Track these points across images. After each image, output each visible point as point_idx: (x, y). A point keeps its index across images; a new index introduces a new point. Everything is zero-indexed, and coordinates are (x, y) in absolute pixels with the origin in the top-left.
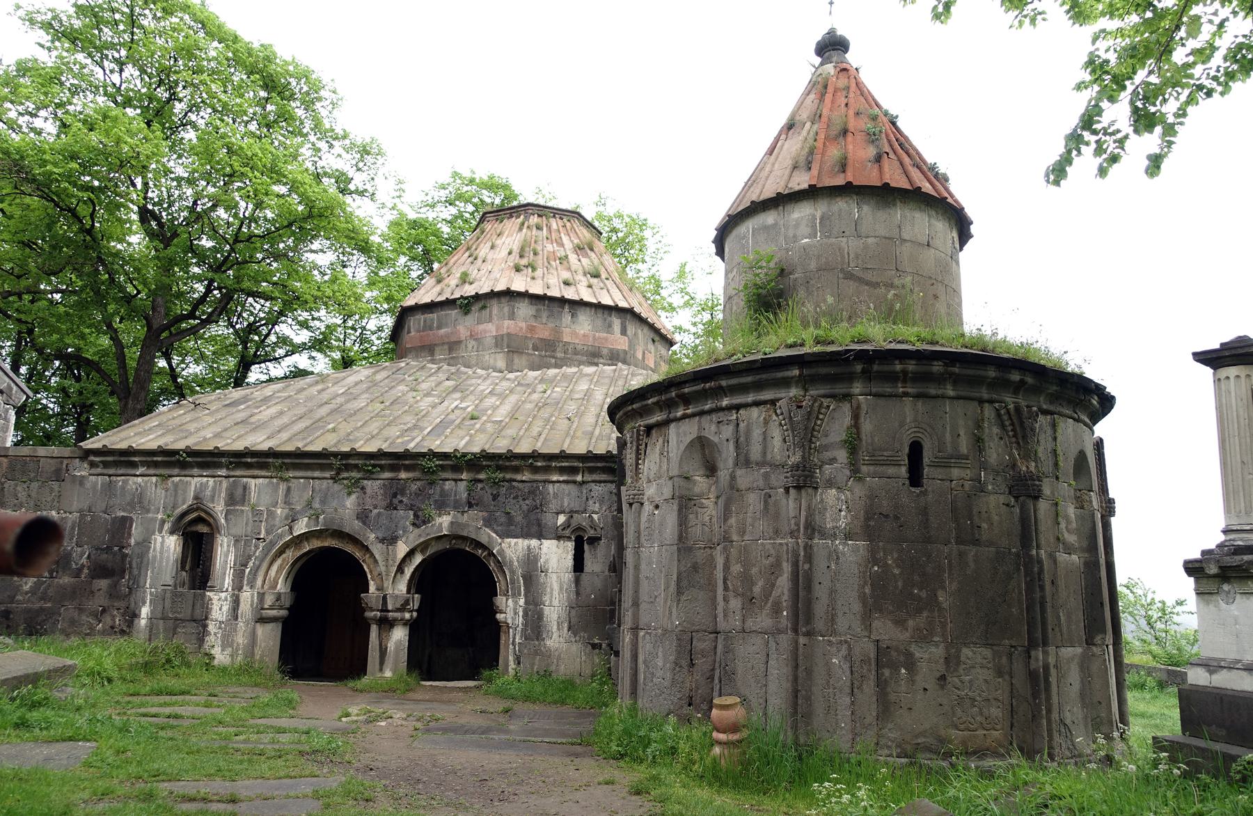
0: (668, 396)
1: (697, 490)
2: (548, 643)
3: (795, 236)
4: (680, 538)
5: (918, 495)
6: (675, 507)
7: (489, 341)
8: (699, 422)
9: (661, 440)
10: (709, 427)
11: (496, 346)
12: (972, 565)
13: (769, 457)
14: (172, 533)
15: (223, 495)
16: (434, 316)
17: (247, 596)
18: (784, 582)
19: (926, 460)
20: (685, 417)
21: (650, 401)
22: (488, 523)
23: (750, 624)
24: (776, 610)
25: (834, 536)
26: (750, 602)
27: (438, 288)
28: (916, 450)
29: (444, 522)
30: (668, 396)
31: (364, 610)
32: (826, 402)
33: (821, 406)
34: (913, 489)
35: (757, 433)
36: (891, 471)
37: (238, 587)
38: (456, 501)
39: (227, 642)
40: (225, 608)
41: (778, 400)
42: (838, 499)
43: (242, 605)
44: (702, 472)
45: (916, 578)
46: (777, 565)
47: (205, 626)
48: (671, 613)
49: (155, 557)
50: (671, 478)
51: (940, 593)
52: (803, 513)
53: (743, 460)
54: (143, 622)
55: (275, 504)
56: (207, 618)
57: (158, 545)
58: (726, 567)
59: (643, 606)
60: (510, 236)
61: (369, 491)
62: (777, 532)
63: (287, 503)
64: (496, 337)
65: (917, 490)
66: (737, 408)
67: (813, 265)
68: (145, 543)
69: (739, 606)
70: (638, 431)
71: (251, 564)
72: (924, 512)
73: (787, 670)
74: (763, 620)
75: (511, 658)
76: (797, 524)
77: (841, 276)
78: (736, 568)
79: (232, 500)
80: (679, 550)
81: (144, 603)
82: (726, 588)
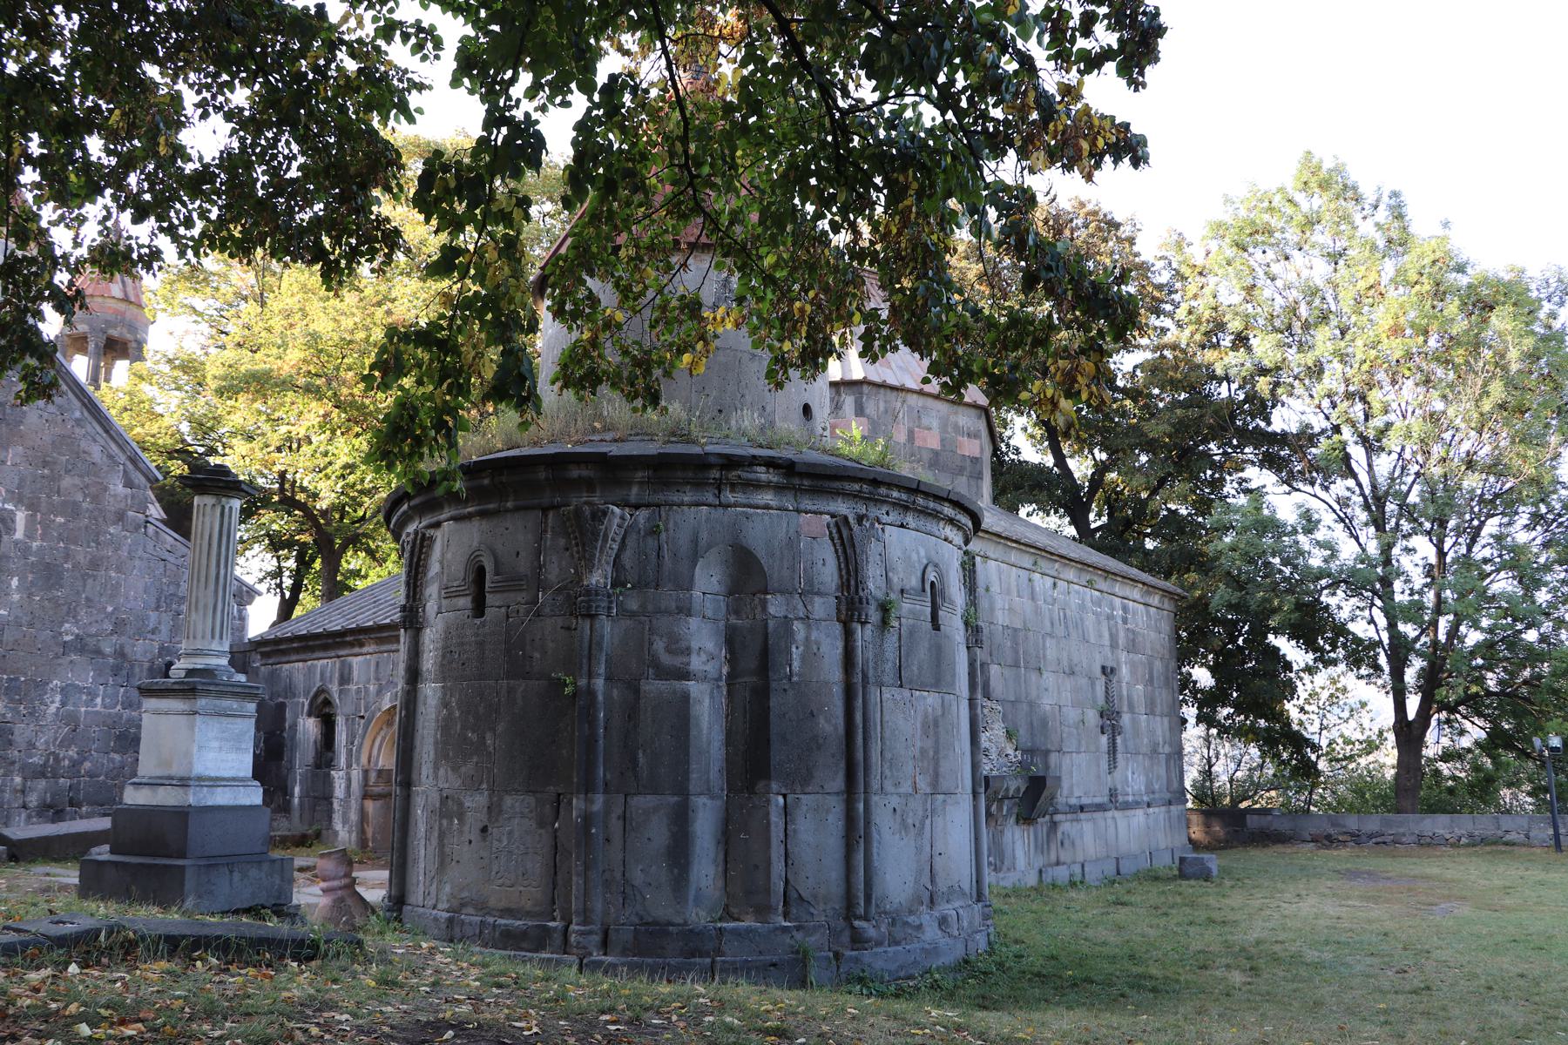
14: (309, 715)
17: (356, 774)
19: (487, 585)
37: (349, 766)
39: (345, 821)
51: (488, 735)
54: (296, 801)
55: (368, 681)
63: (377, 679)
68: (294, 726)
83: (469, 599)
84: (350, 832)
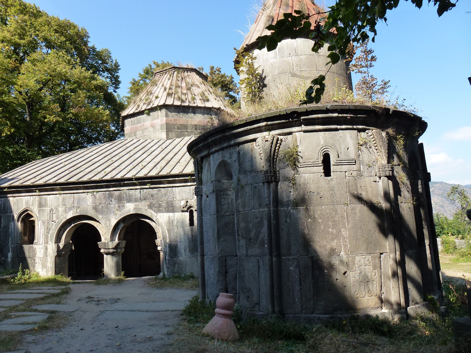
0: (207, 142)
1: (225, 187)
2: (181, 258)
3: (267, 59)
4: (218, 211)
5: (329, 181)
6: (215, 196)
7: (158, 127)
8: (222, 153)
9: (207, 164)
11: (161, 129)
12: (358, 214)
15: (37, 203)
16: (135, 118)
18: (265, 230)
19: (332, 163)
20: (216, 151)
21: (200, 145)
22: (150, 207)
23: (250, 252)
24: (262, 245)
25: (288, 205)
26: (249, 241)
27: (136, 107)
28: (326, 158)
29: (130, 208)
30: (207, 142)
31: (100, 249)
32: (280, 137)
33: (278, 140)
34: (326, 178)
36: (315, 169)
38: (135, 199)
39: (44, 266)
40: (42, 252)
42: (289, 186)
43: (48, 250)
44: (226, 178)
45: (330, 223)
46: (261, 222)
47: (34, 260)
48: (215, 248)
49: (11, 232)
50: (212, 182)
51: (342, 230)
52: (272, 195)
53: (242, 171)
54: (9, 260)
56: (35, 257)
57: (13, 227)
59: (205, 245)
60: (165, 81)
61: (97, 197)
62: (260, 205)
64: (161, 125)
65: (329, 178)
67: (276, 72)
69: (245, 244)
70: (197, 160)
71: (51, 232)
72: (332, 189)
73: (268, 274)
74: (255, 250)
75: (165, 266)
76: (270, 201)
77: (290, 75)
78: (242, 225)
79: (41, 205)
80: (217, 217)
81: (9, 251)
82: (238, 235)
83: (322, 167)
84: (47, 271)
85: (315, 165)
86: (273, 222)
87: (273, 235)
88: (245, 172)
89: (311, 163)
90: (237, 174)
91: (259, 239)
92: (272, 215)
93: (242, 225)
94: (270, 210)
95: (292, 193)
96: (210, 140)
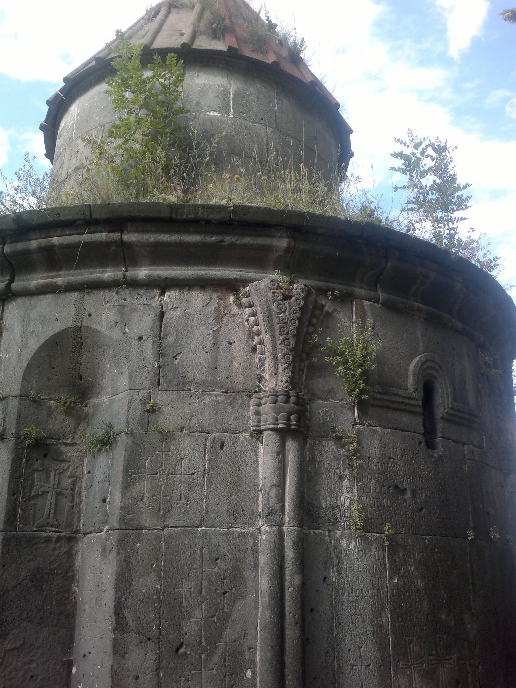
10: (103, 314)
13: (221, 376)
30: (20, 246)
35: (202, 333)
41: (245, 282)
58: (123, 582)
66: (164, 285)
78: (146, 584)
82: (120, 626)
85: (408, 408)
86: (292, 579)
87: (291, 634)
88: (182, 384)
89: (401, 400)
90: (147, 383)
91: (221, 644)
92: (290, 554)
93: (146, 584)
94: (281, 534)
95: (346, 482)
96: (34, 244)
